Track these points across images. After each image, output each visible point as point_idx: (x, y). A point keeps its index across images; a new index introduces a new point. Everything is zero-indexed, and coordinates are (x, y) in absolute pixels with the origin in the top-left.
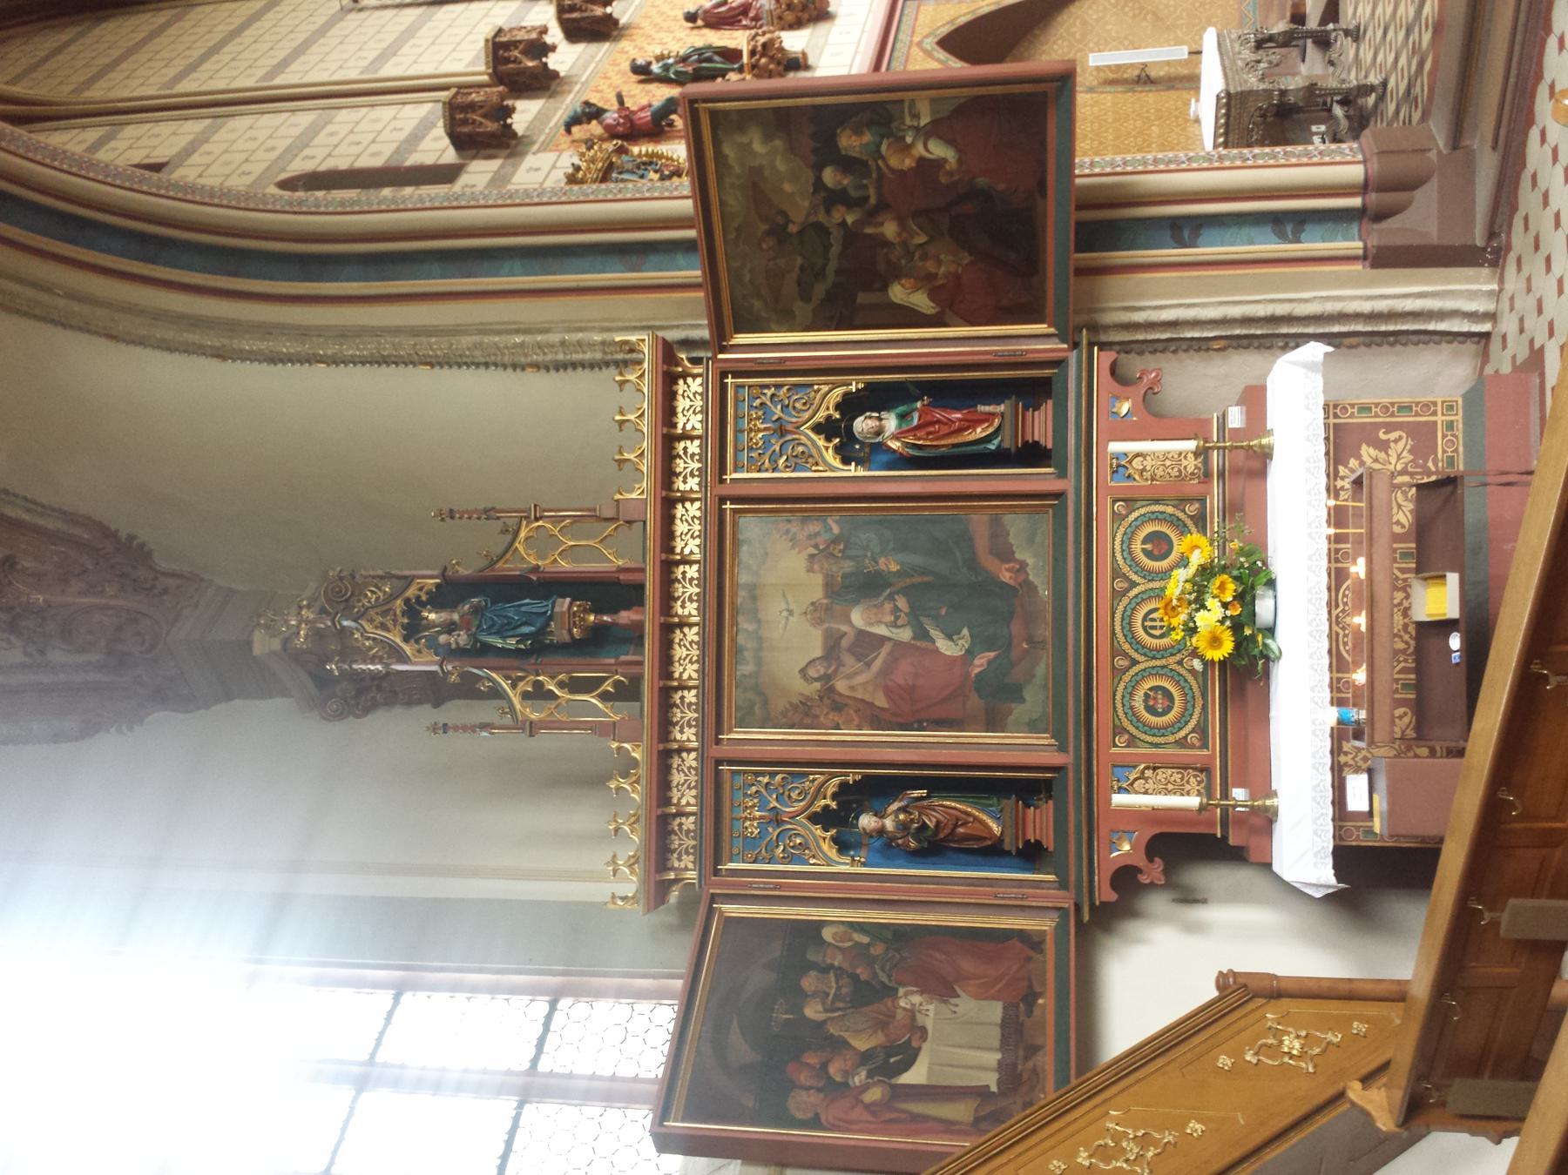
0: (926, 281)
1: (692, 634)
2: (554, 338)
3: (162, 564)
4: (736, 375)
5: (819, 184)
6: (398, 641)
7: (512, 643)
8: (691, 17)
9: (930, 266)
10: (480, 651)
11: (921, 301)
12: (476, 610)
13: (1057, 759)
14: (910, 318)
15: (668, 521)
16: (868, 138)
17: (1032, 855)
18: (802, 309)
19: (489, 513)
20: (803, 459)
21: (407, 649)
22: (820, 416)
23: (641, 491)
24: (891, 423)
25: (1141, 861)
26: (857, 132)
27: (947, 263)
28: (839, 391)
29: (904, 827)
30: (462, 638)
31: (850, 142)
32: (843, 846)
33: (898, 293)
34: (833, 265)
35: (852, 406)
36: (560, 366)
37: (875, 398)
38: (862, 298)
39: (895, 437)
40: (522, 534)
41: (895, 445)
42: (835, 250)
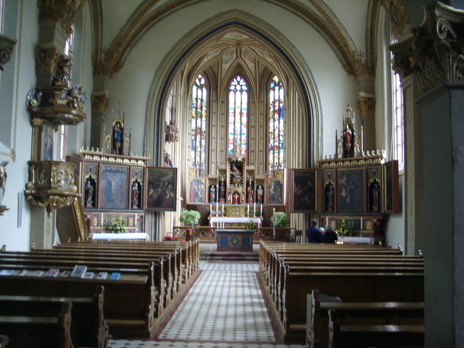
0: (153, 194)
1: (114, 161)
2: (148, 144)
3: (114, 74)
4: (144, 170)
5: (165, 182)
6: (116, 120)
7: (116, 136)
8: (167, 154)
9: (155, 194)
10: (114, 132)
11: (151, 193)
12: (119, 132)
13: (99, 208)
14: (149, 191)
15: (128, 159)
16: (170, 188)
17: (86, 204)
18: (151, 178)
19: (130, 135)
20: (133, 177)
21: (115, 122)
22: (138, 179)
23: (133, 156)
24: (136, 188)
25: (87, 218)
26: (171, 187)
27: (155, 197)
28: (140, 182)
29: (88, 187)
30: (116, 129)
31: (170, 186)
32: (87, 180)
33: (152, 190)
34: (156, 183)
35: (139, 183)
36: (144, 144)
37: (139, 186)
38: (152, 186)
39: (135, 189)
40: (128, 139)
41: (134, 188)
42: (158, 183)
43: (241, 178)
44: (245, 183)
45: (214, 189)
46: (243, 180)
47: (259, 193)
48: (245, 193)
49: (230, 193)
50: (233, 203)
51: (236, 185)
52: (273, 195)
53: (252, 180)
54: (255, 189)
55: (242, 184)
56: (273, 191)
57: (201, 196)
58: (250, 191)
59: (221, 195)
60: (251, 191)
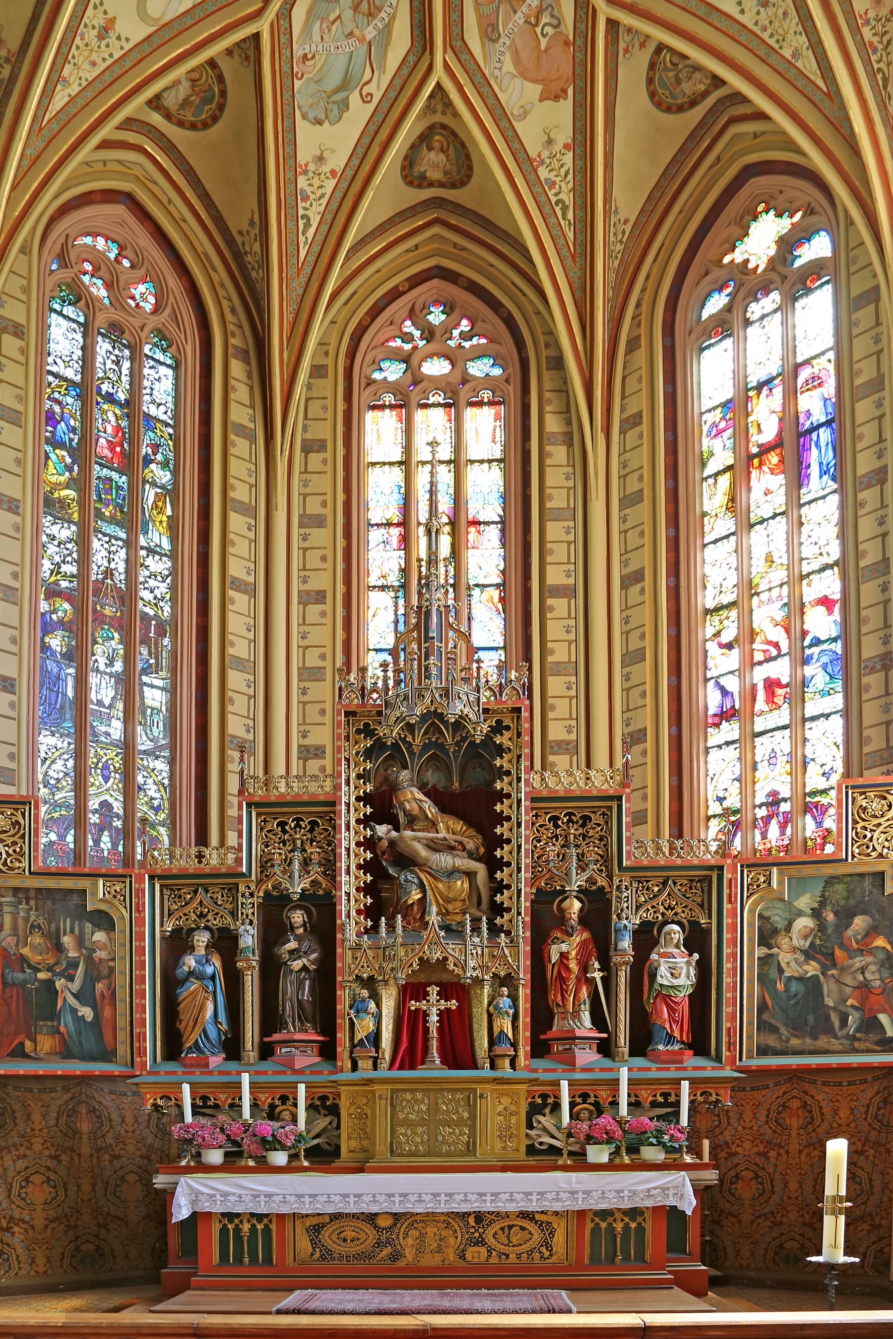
43: (480, 869)
44: (525, 904)
45: (216, 961)
46: (499, 887)
47: (664, 977)
48: (524, 976)
49: (370, 983)
50: (390, 1069)
51: (434, 918)
52: (813, 986)
53: (591, 881)
54: (626, 943)
55: (498, 909)
56: (809, 954)
57: (87, 1013)
58: (573, 965)
59: (288, 1009)
60: (585, 968)
